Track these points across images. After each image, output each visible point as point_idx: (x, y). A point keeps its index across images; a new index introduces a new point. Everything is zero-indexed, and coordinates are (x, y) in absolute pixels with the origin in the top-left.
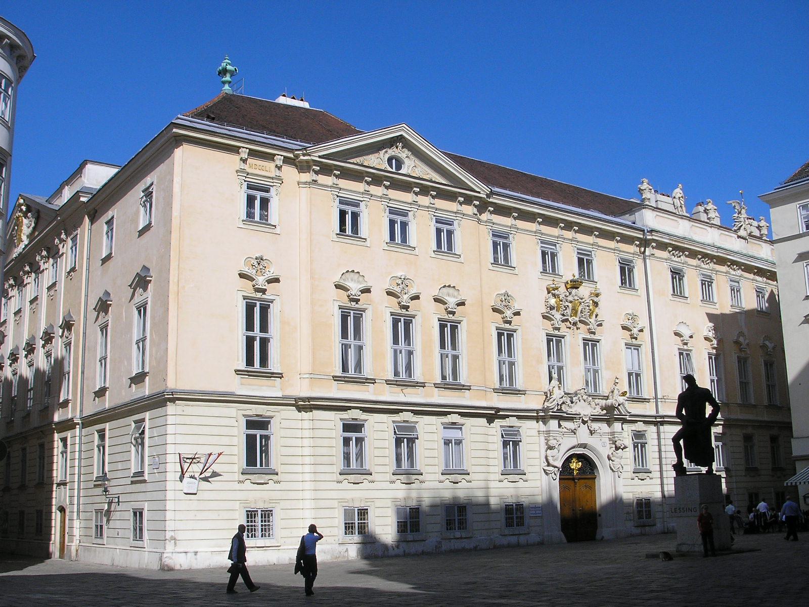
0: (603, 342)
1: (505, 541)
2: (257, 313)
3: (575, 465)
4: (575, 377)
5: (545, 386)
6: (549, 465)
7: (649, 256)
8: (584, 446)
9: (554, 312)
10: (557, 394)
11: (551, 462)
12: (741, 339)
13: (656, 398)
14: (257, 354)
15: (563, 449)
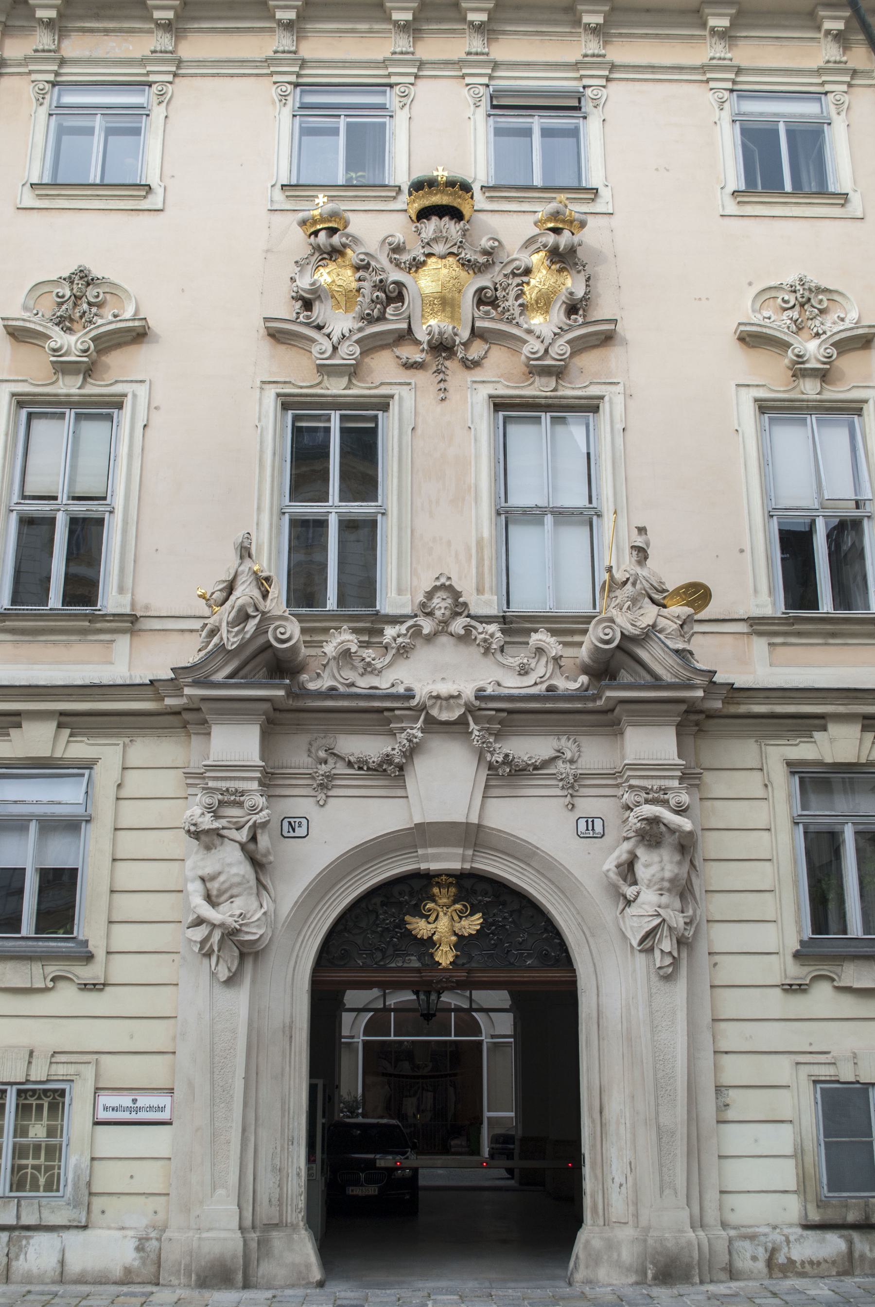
8: (472, 835)
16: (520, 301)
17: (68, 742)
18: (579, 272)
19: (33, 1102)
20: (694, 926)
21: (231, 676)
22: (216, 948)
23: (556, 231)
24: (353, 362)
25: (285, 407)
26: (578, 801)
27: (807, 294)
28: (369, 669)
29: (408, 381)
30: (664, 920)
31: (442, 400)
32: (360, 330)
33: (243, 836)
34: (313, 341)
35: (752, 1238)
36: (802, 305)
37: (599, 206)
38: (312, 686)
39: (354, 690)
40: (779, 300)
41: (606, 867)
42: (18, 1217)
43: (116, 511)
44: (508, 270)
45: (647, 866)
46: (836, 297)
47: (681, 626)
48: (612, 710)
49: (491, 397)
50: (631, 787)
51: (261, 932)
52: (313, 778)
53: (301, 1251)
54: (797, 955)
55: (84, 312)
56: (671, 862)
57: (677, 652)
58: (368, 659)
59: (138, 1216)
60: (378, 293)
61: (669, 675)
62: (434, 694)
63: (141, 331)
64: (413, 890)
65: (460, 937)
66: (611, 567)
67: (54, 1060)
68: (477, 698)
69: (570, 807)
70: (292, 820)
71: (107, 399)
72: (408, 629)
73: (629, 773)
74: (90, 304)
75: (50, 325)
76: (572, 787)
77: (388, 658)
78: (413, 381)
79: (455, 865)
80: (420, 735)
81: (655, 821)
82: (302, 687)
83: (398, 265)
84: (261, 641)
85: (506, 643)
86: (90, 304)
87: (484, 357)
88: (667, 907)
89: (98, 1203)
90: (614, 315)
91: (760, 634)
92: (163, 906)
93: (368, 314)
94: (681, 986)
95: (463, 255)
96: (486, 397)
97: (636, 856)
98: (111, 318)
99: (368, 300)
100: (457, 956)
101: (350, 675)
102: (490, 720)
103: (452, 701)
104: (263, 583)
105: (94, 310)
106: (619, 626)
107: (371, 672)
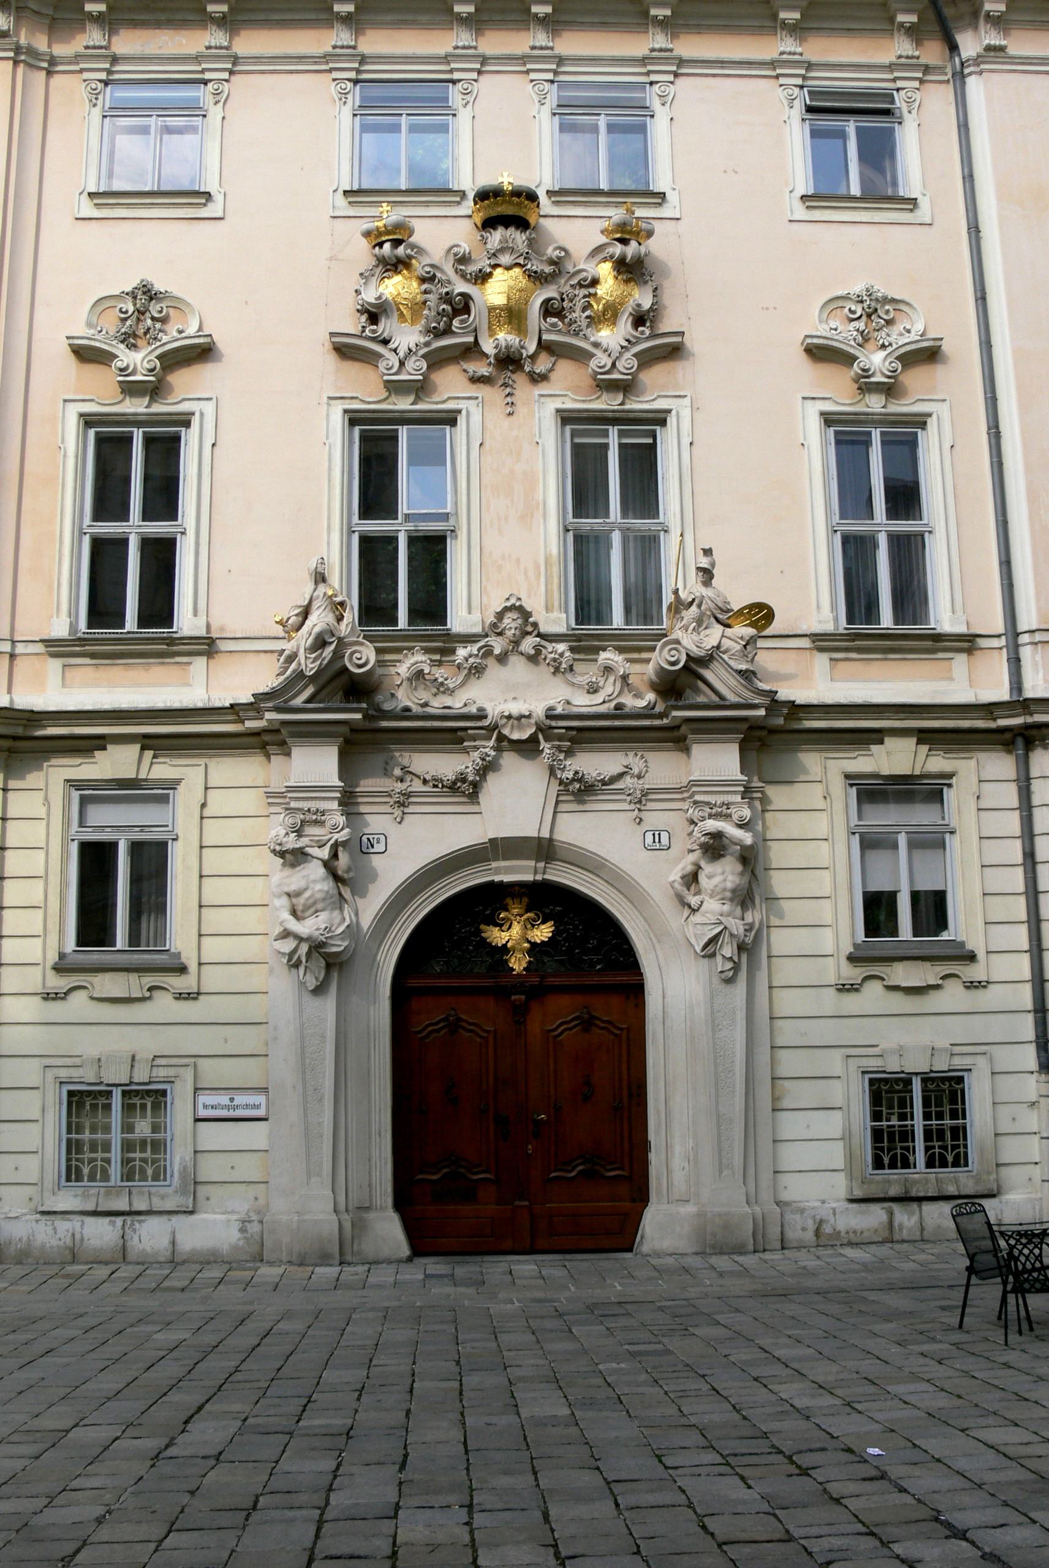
1: (49, 1236)
7: (978, 60)
8: (544, 849)
13: (1013, 632)
16: (588, 313)
17: (152, 763)
18: (646, 282)
19: (137, 1101)
20: (753, 933)
21: (308, 701)
22: (304, 960)
23: (624, 241)
24: (421, 377)
25: (353, 422)
26: (643, 815)
27: (873, 304)
28: (442, 689)
29: (475, 395)
30: (725, 928)
31: (510, 414)
32: (427, 344)
33: (325, 853)
34: (379, 356)
35: (802, 1211)
36: (869, 316)
37: (666, 212)
38: (387, 706)
39: (429, 710)
40: (846, 310)
41: (671, 878)
42: (130, 1205)
43: (188, 532)
44: (574, 281)
45: (710, 877)
46: (902, 307)
47: (745, 646)
48: (678, 727)
49: (558, 411)
50: (695, 802)
51: (346, 944)
52: (390, 796)
53: (389, 1231)
54: (851, 959)
55: (149, 329)
56: (733, 874)
57: (740, 672)
58: (441, 680)
59: (241, 1203)
60: (444, 306)
61: (733, 695)
62: (506, 714)
63: (207, 346)
64: (489, 901)
65: (534, 945)
66: (678, 589)
67: (155, 1063)
68: (548, 717)
69: (638, 820)
70: (371, 837)
71: (175, 418)
72: (479, 650)
73: (694, 789)
74: (153, 319)
75: (114, 343)
76: (640, 802)
77: (460, 679)
78: (480, 396)
79: (529, 877)
80: (493, 753)
81: (718, 836)
82: (379, 709)
83: (463, 276)
84: (337, 666)
85: (574, 660)
86: (153, 319)
87: (551, 370)
88: (728, 915)
89: (202, 1190)
90: (681, 325)
91: (821, 650)
92: (250, 920)
93: (434, 328)
94: (740, 987)
95: (529, 267)
96: (553, 411)
97: (700, 868)
98: (175, 334)
99: (433, 313)
100: (529, 962)
101: (424, 695)
102: (560, 738)
103: (523, 720)
104: (338, 608)
105: (158, 325)
106: (684, 647)
107: (444, 693)
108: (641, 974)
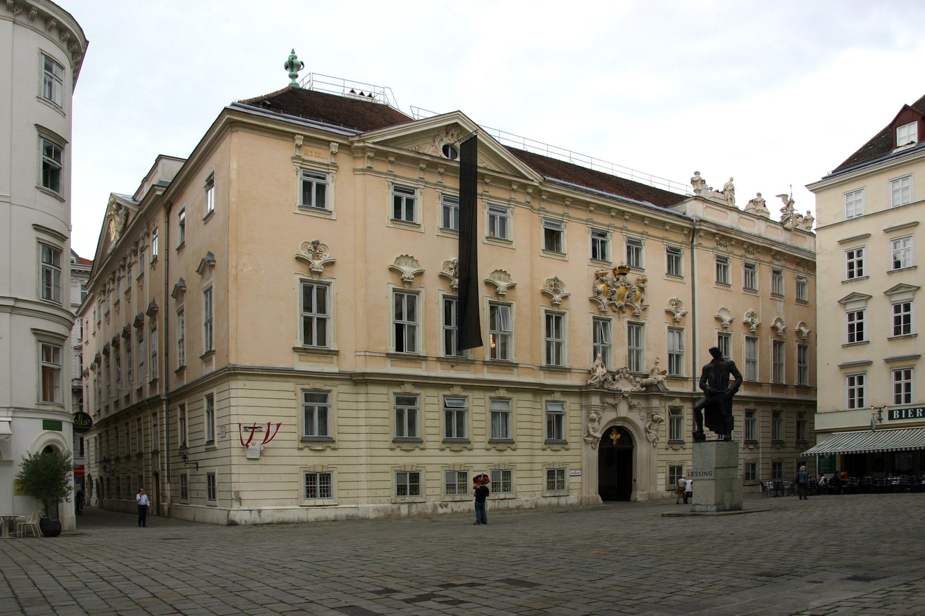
0: (647, 326)
2: (314, 296)
3: (615, 437)
4: (618, 358)
5: (589, 363)
6: (589, 435)
8: (624, 419)
9: (601, 297)
10: (600, 371)
11: (592, 433)
12: (779, 325)
14: (314, 330)
15: (604, 422)
108: (633, 447)
